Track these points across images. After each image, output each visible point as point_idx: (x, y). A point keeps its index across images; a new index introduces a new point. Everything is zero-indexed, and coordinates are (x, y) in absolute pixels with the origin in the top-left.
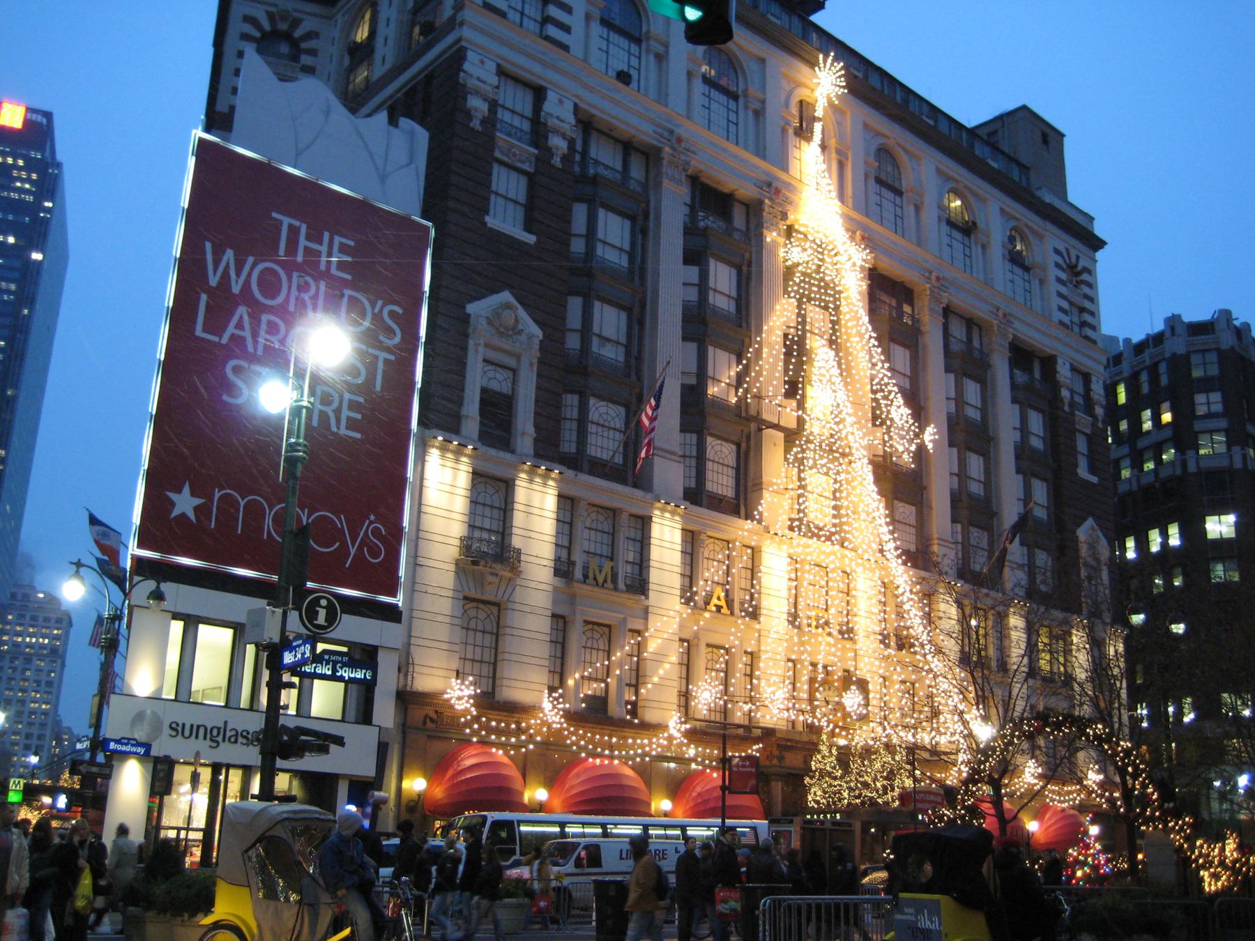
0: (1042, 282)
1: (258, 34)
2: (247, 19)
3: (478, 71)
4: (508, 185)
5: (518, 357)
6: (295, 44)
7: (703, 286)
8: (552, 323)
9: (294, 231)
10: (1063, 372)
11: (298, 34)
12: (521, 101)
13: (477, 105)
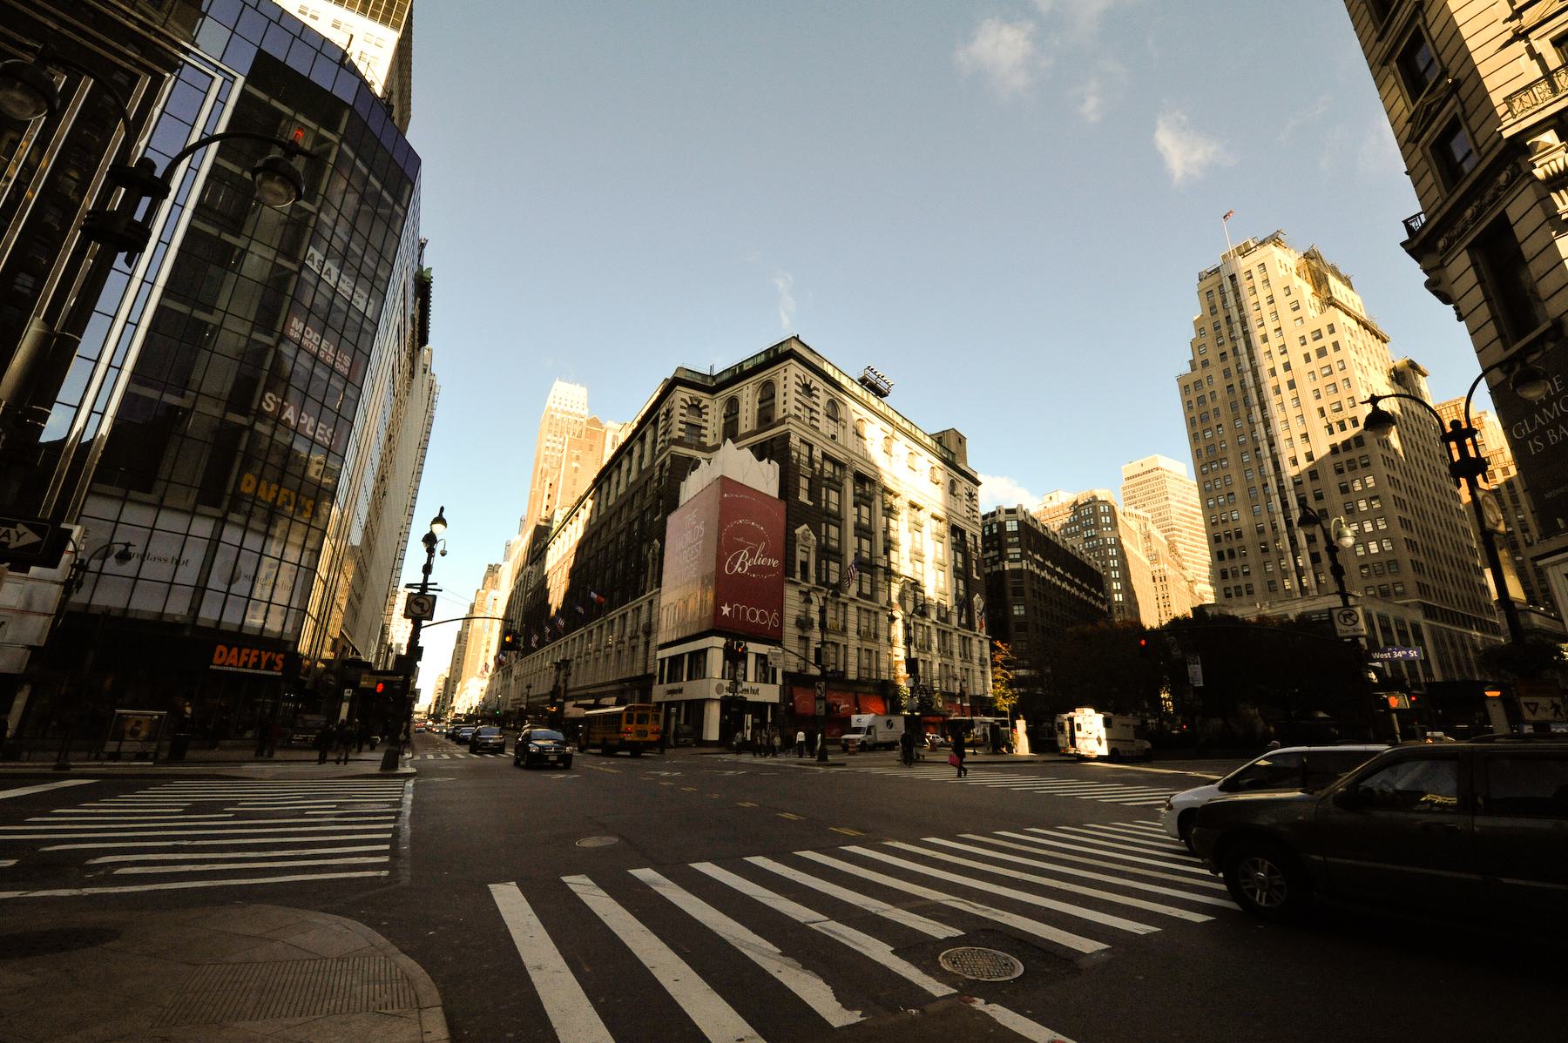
3: (794, 441)
4: (804, 483)
7: (859, 516)
8: (818, 534)
10: (968, 535)
12: (805, 450)
13: (794, 454)
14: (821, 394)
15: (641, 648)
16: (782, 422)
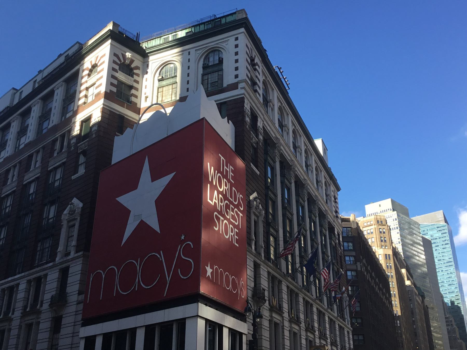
0: (330, 201)
1: (119, 63)
2: (115, 55)
3: (247, 106)
5: (258, 217)
6: (132, 70)
9: (223, 161)
11: (133, 66)
14: (260, 71)
15: (45, 325)
16: (234, 86)
